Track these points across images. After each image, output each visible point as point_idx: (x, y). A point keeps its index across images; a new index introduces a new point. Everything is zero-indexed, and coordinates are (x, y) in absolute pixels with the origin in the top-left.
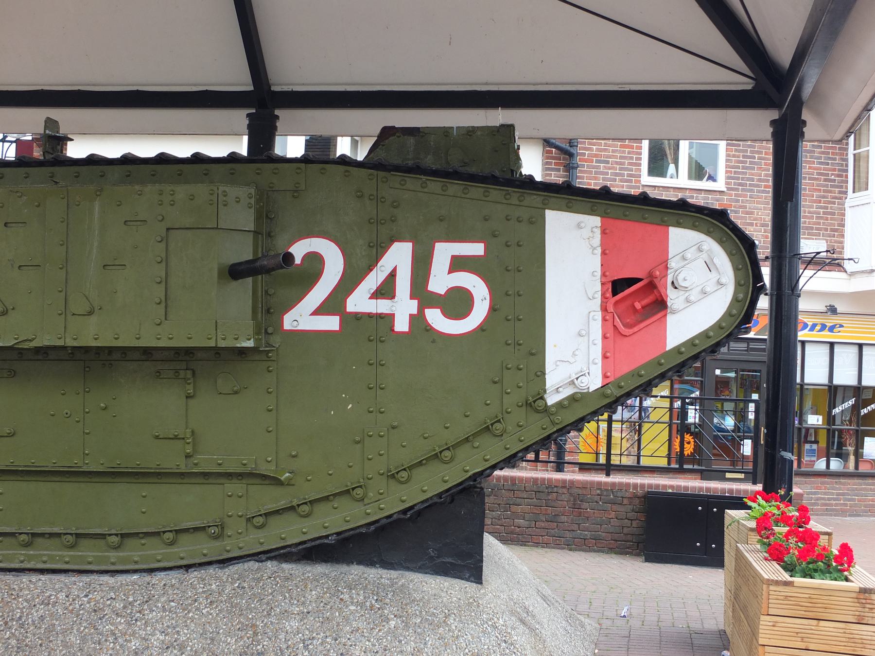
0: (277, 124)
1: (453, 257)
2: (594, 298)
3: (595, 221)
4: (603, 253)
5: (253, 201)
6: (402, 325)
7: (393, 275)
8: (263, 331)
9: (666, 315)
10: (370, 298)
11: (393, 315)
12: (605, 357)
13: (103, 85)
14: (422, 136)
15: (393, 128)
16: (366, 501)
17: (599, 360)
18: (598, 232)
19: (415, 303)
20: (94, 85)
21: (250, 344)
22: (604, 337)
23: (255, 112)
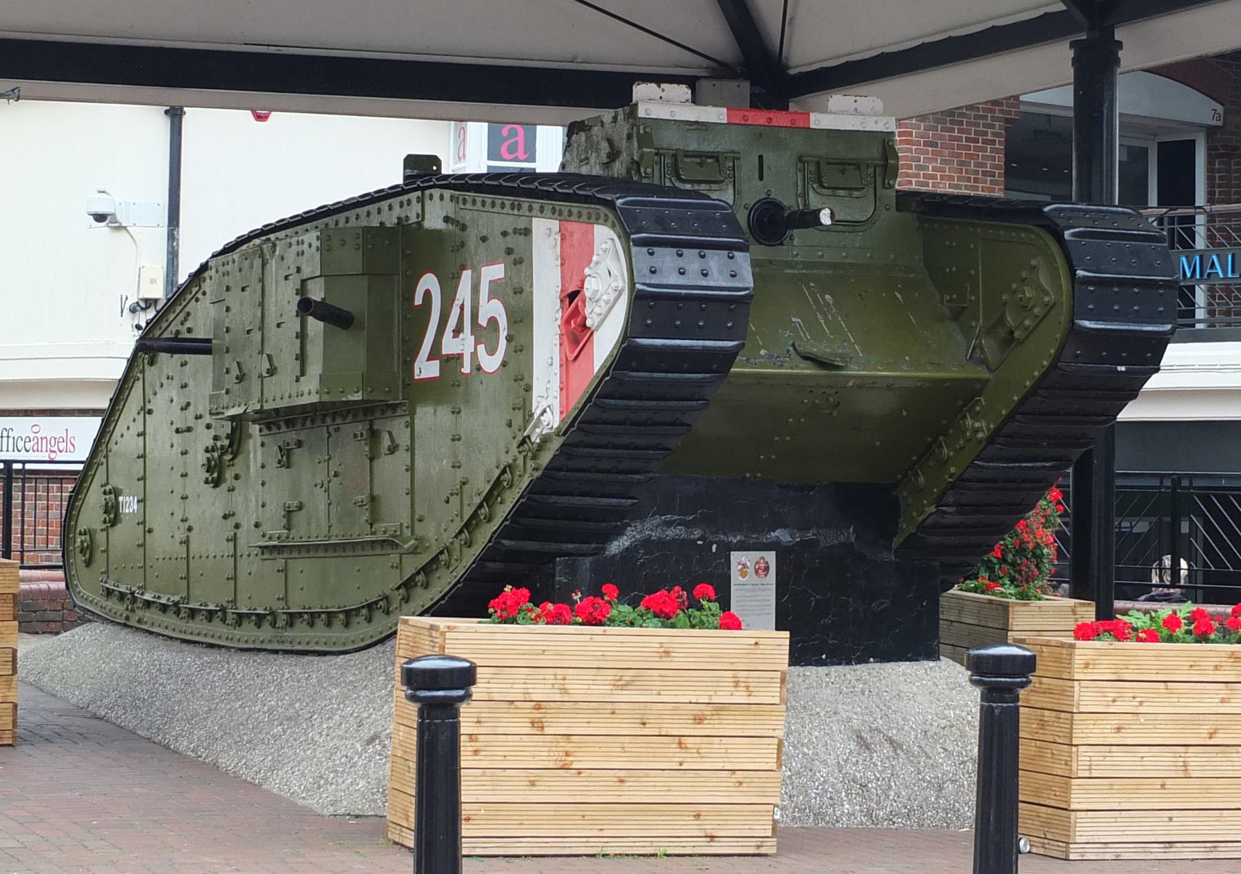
0: (1120, 54)
1: (491, 282)
2: (556, 320)
3: (555, 224)
4: (562, 265)
5: (360, 241)
6: (466, 369)
7: (462, 308)
8: (400, 383)
9: (592, 333)
10: (453, 337)
11: (462, 354)
12: (561, 389)
13: (968, 25)
14: (589, 130)
15: (576, 122)
16: (451, 569)
17: (557, 394)
18: (558, 237)
19: (473, 337)
20: (962, 26)
21: (358, 397)
22: (561, 366)
23: (1085, 37)
